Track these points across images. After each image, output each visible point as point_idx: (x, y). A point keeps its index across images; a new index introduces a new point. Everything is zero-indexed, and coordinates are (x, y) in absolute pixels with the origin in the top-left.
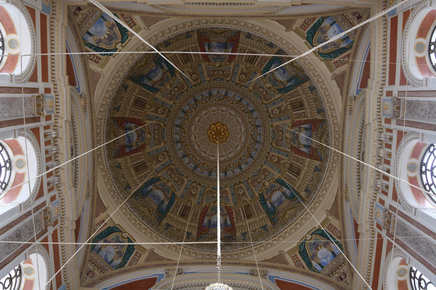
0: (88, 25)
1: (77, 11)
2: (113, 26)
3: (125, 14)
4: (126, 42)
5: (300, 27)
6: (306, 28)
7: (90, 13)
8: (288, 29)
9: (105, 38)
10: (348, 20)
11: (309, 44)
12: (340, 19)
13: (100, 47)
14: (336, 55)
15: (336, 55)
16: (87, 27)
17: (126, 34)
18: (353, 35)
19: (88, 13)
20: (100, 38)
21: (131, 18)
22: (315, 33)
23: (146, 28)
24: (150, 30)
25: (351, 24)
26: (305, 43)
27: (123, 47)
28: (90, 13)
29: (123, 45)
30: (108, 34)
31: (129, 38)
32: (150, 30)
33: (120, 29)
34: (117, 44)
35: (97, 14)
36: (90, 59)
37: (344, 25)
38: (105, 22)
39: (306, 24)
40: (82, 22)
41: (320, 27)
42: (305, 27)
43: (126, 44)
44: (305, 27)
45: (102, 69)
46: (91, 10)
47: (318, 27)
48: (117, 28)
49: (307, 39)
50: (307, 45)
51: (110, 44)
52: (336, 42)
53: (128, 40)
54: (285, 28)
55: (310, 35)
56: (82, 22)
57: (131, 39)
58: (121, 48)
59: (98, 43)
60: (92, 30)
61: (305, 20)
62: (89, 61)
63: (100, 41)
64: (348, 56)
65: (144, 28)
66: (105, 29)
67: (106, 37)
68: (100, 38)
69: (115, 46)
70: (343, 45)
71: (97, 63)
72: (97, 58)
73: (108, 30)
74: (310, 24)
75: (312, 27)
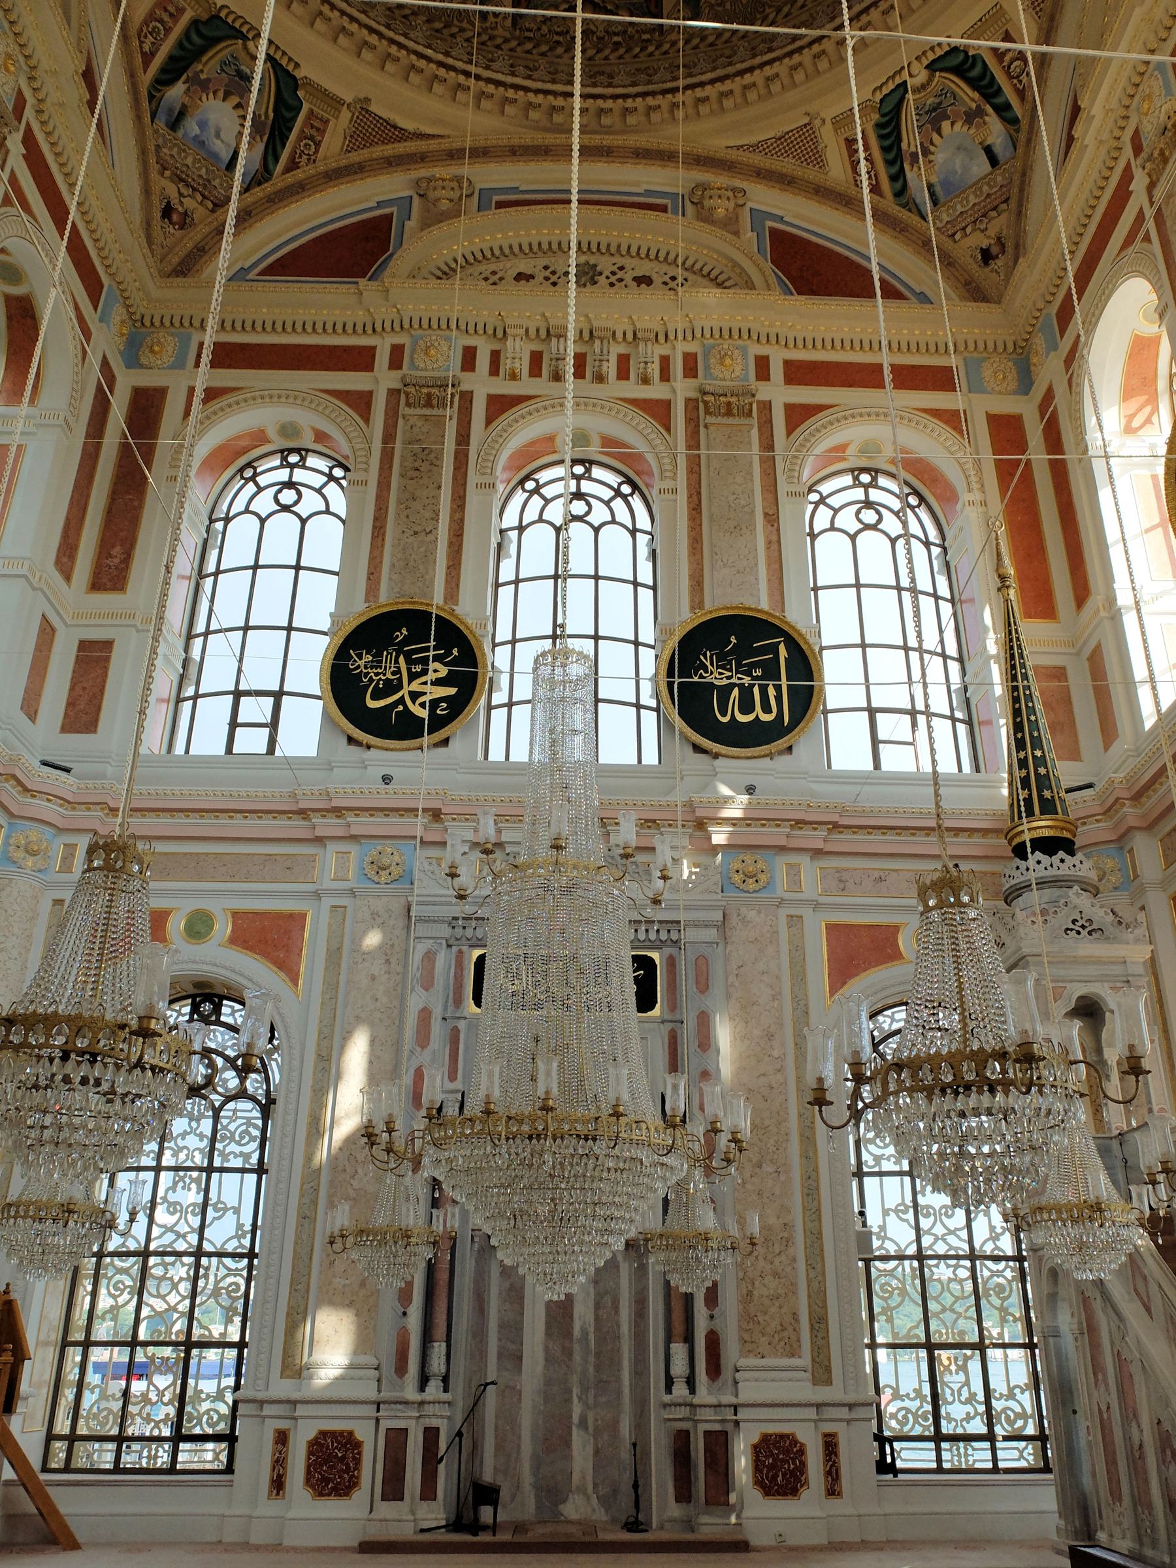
0: (985, 188)
4: (891, 86)
5: (327, 122)
6: (308, 122)
7: (964, 229)
8: (362, 107)
9: (953, 124)
10: (194, 189)
11: (284, 62)
12: (216, 182)
13: (976, 95)
14: (186, 44)
15: (186, 44)
16: (988, 184)
17: (883, 116)
18: (160, 141)
19: (968, 230)
20: (965, 128)
22: (275, 110)
23: (817, 122)
24: (807, 114)
25: (182, 180)
26: (297, 65)
28: (964, 229)
30: (939, 132)
32: (807, 114)
33: (899, 139)
34: (924, 87)
35: (945, 218)
37: (199, 169)
39: (312, 138)
40: (995, 209)
41: (265, 138)
42: (312, 127)
43: (893, 77)
44: (312, 127)
46: (957, 237)
47: (271, 135)
48: (904, 145)
49: (294, 83)
50: (290, 59)
51: (943, 93)
52: (204, 98)
53: (885, 91)
54: (373, 108)
55: (290, 101)
56: (995, 209)
57: (875, 90)
59: (980, 112)
60: (982, 165)
61: (316, 151)
63: (971, 117)
64: (148, 58)
65: (824, 121)
66: (939, 157)
67: (945, 125)
68: (965, 128)
69: (930, 80)
70: (176, 92)
73: (932, 148)
74: (300, 138)
75: (290, 130)
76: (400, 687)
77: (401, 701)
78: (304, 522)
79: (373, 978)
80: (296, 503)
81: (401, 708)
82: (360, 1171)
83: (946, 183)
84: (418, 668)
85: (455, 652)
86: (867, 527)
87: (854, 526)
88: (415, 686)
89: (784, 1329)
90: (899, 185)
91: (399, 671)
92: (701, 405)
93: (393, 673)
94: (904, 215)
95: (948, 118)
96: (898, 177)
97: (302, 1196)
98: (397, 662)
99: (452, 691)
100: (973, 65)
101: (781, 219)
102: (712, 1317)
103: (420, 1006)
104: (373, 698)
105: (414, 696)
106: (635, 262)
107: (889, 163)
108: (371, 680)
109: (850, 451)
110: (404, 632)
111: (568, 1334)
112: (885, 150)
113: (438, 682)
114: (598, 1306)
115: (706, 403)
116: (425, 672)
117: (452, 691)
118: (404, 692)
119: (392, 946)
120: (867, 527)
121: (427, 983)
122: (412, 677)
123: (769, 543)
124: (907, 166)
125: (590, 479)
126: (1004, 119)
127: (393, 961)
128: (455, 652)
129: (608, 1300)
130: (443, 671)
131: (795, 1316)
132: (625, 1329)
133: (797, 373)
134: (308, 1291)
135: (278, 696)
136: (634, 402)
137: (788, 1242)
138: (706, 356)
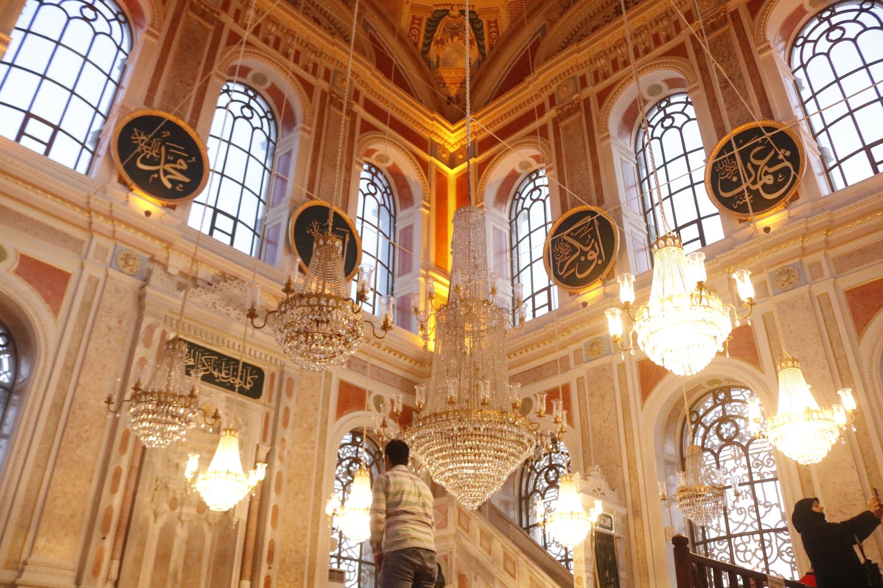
1: (454, 100)
2: (437, 43)
3: (411, 45)
4: (442, 8)
21: (411, 30)
27: (452, 6)
29: (449, 8)
30: (452, 39)
31: (435, 8)
33: (434, 31)
34: (455, 17)
36: (498, 34)
38: (441, 56)
43: (445, 5)
45: (501, 9)
48: (435, 35)
53: (439, 8)
58: (455, 8)
62: (501, 34)
66: (448, 49)
67: (456, 38)
71: (496, 22)
72: (491, 27)
76: (158, 164)
77: (158, 172)
78: (96, 34)
79: (110, 329)
80: (94, 20)
81: (156, 176)
82: (83, 444)
83: (444, 60)
84: (171, 158)
85: (194, 159)
86: (370, 193)
87: (366, 191)
88: (168, 167)
89: (297, 580)
90: (425, 49)
91: (159, 154)
92: (328, 98)
93: (157, 154)
94: (423, 63)
95: (458, 36)
96: (427, 45)
97: (39, 451)
98: (160, 148)
99: (187, 180)
100: (478, 23)
101: (375, 31)
102: (270, 568)
103: (141, 355)
104: (142, 162)
105: (166, 173)
106: (315, 10)
107: (426, 38)
108: (143, 151)
109: (374, 156)
110: (168, 133)
111: (167, 571)
112: (427, 31)
113: (181, 171)
114: (187, 557)
115: (332, 97)
116: (175, 162)
117: (187, 180)
118: (161, 167)
119: (125, 313)
120: (370, 193)
121: (147, 345)
122: (167, 162)
123: (345, 181)
124: (432, 44)
125: (255, 100)
126: (480, 51)
127: (124, 323)
128: (194, 159)
129: (195, 554)
130: (185, 167)
131: (303, 574)
132: (204, 571)
133: (370, 107)
134: (32, 514)
135: (57, 129)
136: (298, 77)
137: (305, 536)
138: (335, 75)
